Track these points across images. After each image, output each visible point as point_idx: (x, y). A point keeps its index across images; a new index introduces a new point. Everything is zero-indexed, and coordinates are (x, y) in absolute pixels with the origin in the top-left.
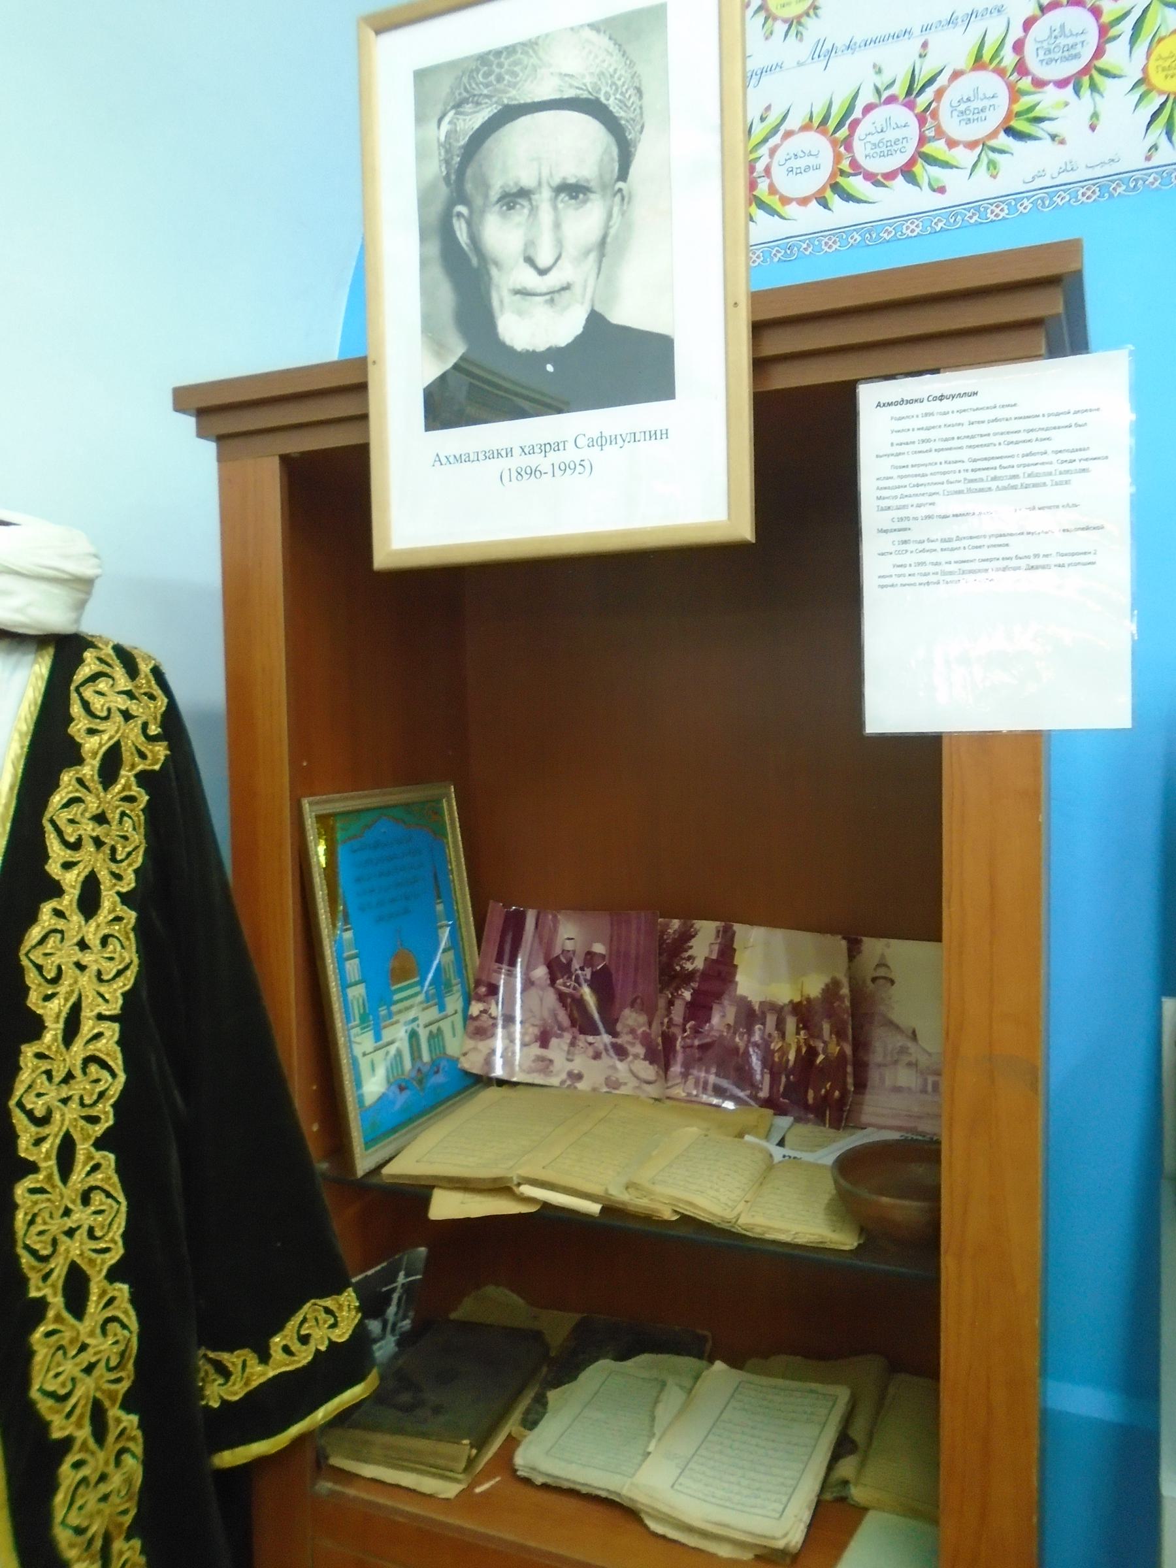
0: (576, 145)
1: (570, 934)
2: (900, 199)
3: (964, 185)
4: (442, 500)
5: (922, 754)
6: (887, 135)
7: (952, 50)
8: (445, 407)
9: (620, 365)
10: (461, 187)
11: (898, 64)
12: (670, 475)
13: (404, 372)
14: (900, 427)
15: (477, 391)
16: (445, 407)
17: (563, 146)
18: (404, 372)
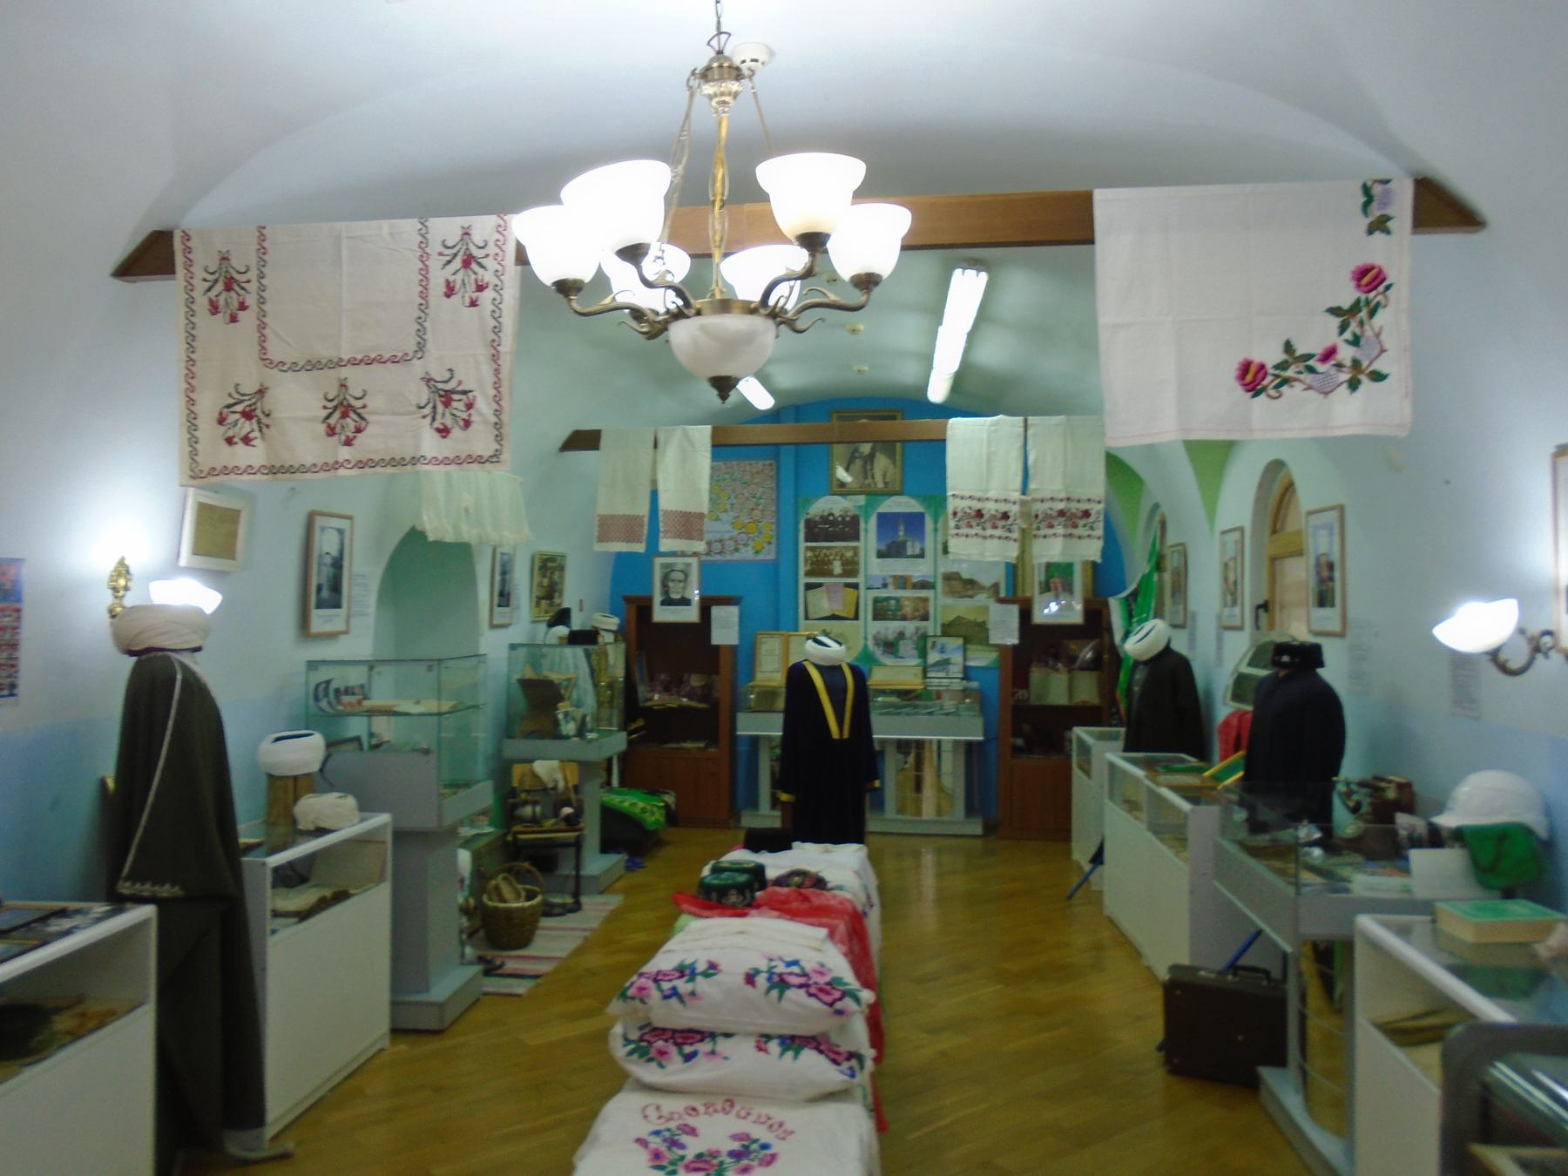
0: (680, 576)
1: (663, 677)
2: (718, 557)
3: (728, 557)
4: (662, 614)
5: (717, 647)
6: (717, 547)
7: (727, 536)
8: (663, 603)
9: (685, 602)
10: (665, 579)
11: (718, 536)
12: (691, 615)
13: (658, 598)
14: (717, 612)
15: (668, 602)
16: (663, 603)
17: (680, 576)
18: (658, 598)
